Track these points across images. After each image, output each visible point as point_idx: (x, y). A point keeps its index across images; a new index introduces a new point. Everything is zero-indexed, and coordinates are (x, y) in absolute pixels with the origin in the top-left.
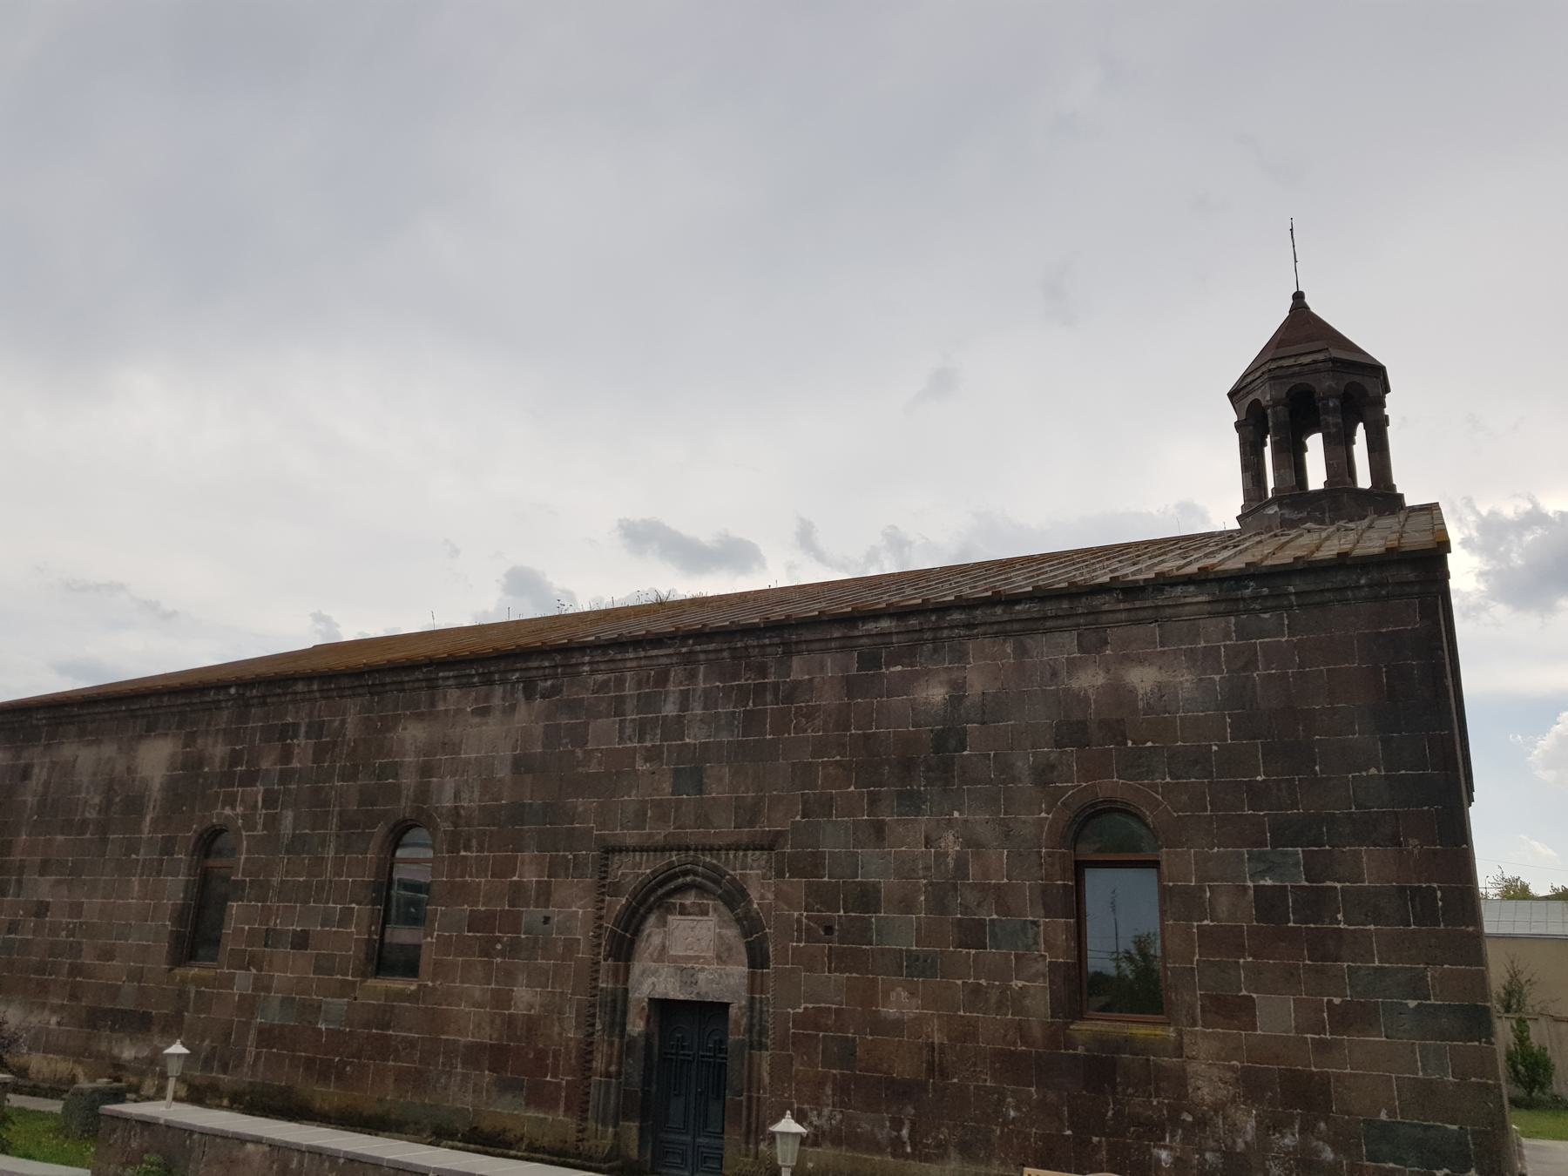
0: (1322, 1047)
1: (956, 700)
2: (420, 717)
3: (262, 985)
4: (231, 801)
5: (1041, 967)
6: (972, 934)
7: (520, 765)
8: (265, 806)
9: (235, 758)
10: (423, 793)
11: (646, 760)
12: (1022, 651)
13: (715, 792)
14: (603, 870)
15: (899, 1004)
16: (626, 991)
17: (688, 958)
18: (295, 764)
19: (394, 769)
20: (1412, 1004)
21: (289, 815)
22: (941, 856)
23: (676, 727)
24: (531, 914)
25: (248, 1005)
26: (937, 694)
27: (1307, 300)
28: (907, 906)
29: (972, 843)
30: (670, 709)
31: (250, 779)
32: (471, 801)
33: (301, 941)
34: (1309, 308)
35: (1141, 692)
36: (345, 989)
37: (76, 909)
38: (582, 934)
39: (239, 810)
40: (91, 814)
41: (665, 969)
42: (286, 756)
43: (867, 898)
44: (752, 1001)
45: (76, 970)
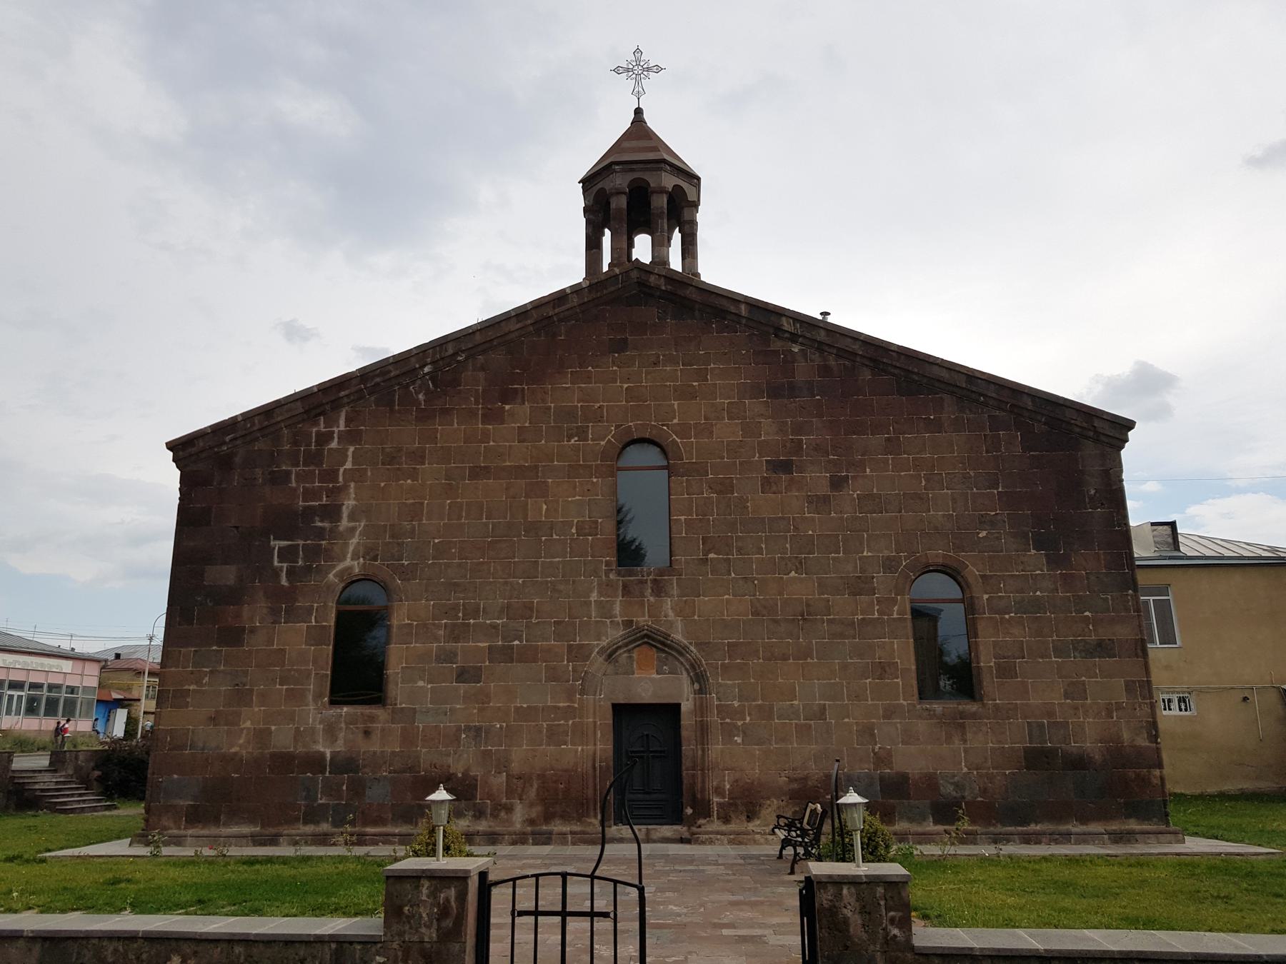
27: (646, 116)
34: (646, 123)
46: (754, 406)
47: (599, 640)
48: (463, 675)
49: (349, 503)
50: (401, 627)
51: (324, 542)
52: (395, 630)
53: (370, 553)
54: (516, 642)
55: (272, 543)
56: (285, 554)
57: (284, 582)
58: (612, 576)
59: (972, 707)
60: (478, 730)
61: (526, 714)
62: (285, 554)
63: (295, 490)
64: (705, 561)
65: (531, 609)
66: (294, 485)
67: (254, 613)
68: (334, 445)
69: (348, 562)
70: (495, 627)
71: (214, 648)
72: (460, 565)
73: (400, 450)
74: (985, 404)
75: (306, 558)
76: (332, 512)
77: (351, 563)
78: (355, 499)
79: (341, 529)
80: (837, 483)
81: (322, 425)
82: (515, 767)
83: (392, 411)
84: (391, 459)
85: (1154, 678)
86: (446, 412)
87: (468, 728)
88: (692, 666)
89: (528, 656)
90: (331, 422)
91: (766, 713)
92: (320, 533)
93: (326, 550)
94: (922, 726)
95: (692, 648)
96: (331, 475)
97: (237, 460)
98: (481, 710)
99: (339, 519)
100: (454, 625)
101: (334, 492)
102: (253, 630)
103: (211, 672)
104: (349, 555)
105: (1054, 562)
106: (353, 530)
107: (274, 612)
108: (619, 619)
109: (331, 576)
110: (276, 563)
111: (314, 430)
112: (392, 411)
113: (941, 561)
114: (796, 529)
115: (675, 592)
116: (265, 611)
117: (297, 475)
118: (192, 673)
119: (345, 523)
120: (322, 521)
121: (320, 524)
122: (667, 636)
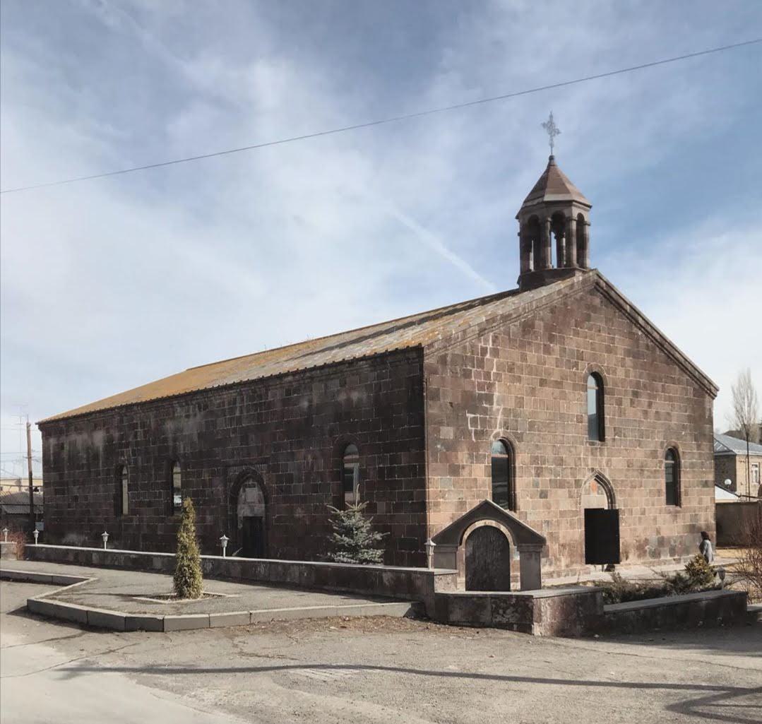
0: (392, 517)
1: (310, 406)
2: (171, 419)
3: (141, 520)
4: (122, 454)
5: (330, 498)
6: (315, 489)
7: (200, 436)
8: (133, 456)
9: (121, 438)
10: (175, 448)
11: (233, 433)
12: (326, 386)
13: (252, 444)
14: (225, 473)
15: (299, 513)
16: (237, 515)
17: (252, 502)
18: (139, 439)
19: (165, 440)
20: (410, 502)
21: (140, 458)
22: (308, 463)
23: (239, 420)
24: (208, 490)
25: (139, 527)
26: (305, 404)
28: (300, 480)
29: (314, 458)
30: (238, 414)
31: (127, 445)
32: (189, 451)
33: (149, 504)
35: (354, 402)
36: (162, 520)
37: (86, 498)
38: (222, 497)
39: (126, 457)
40: (85, 462)
41: (246, 507)
42: (136, 436)
43: (290, 478)
44: (266, 515)
45: (90, 520)
46: (629, 361)
47: (584, 477)
48: (543, 495)
49: (496, 394)
50: (519, 467)
51: (488, 417)
52: (517, 470)
53: (506, 425)
54: (558, 478)
55: (467, 415)
56: (474, 421)
57: (474, 440)
58: (588, 445)
59: (678, 508)
60: (548, 522)
61: (563, 514)
62: (474, 421)
63: (473, 382)
64: (614, 439)
65: (562, 460)
66: (473, 379)
67: (462, 457)
68: (488, 356)
69: (498, 430)
70: (551, 469)
71: (448, 477)
72: (539, 435)
73: (513, 364)
74: (686, 373)
75: (481, 427)
76: (489, 398)
77: (499, 430)
78: (498, 392)
79: (494, 409)
80: (650, 405)
81: (482, 343)
82: (562, 541)
83: (509, 338)
84: (511, 370)
85: (716, 497)
86: (529, 343)
87: (545, 522)
88: (610, 491)
89: (561, 485)
90: (486, 341)
91: (631, 512)
92: (485, 411)
93: (489, 421)
94: (668, 516)
95: (611, 482)
96: (488, 375)
97: (449, 359)
98: (549, 513)
99: (492, 404)
100: (538, 468)
101: (491, 386)
102: (463, 467)
103: (449, 491)
104: (498, 426)
105: (699, 447)
106: (498, 410)
107: (471, 456)
108: (590, 467)
109: (492, 437)
110: (470, 428)
111: (480, 345)
112: (509, 338)
113: (673, 444)
114: (639, 426)
115: (606, 453)
116: (467, 456)
117: (474, 373)
118: (440, 491)
119: (495, 407)
120: (486, 404)
121: (485, 405)
122: (604, 476)
